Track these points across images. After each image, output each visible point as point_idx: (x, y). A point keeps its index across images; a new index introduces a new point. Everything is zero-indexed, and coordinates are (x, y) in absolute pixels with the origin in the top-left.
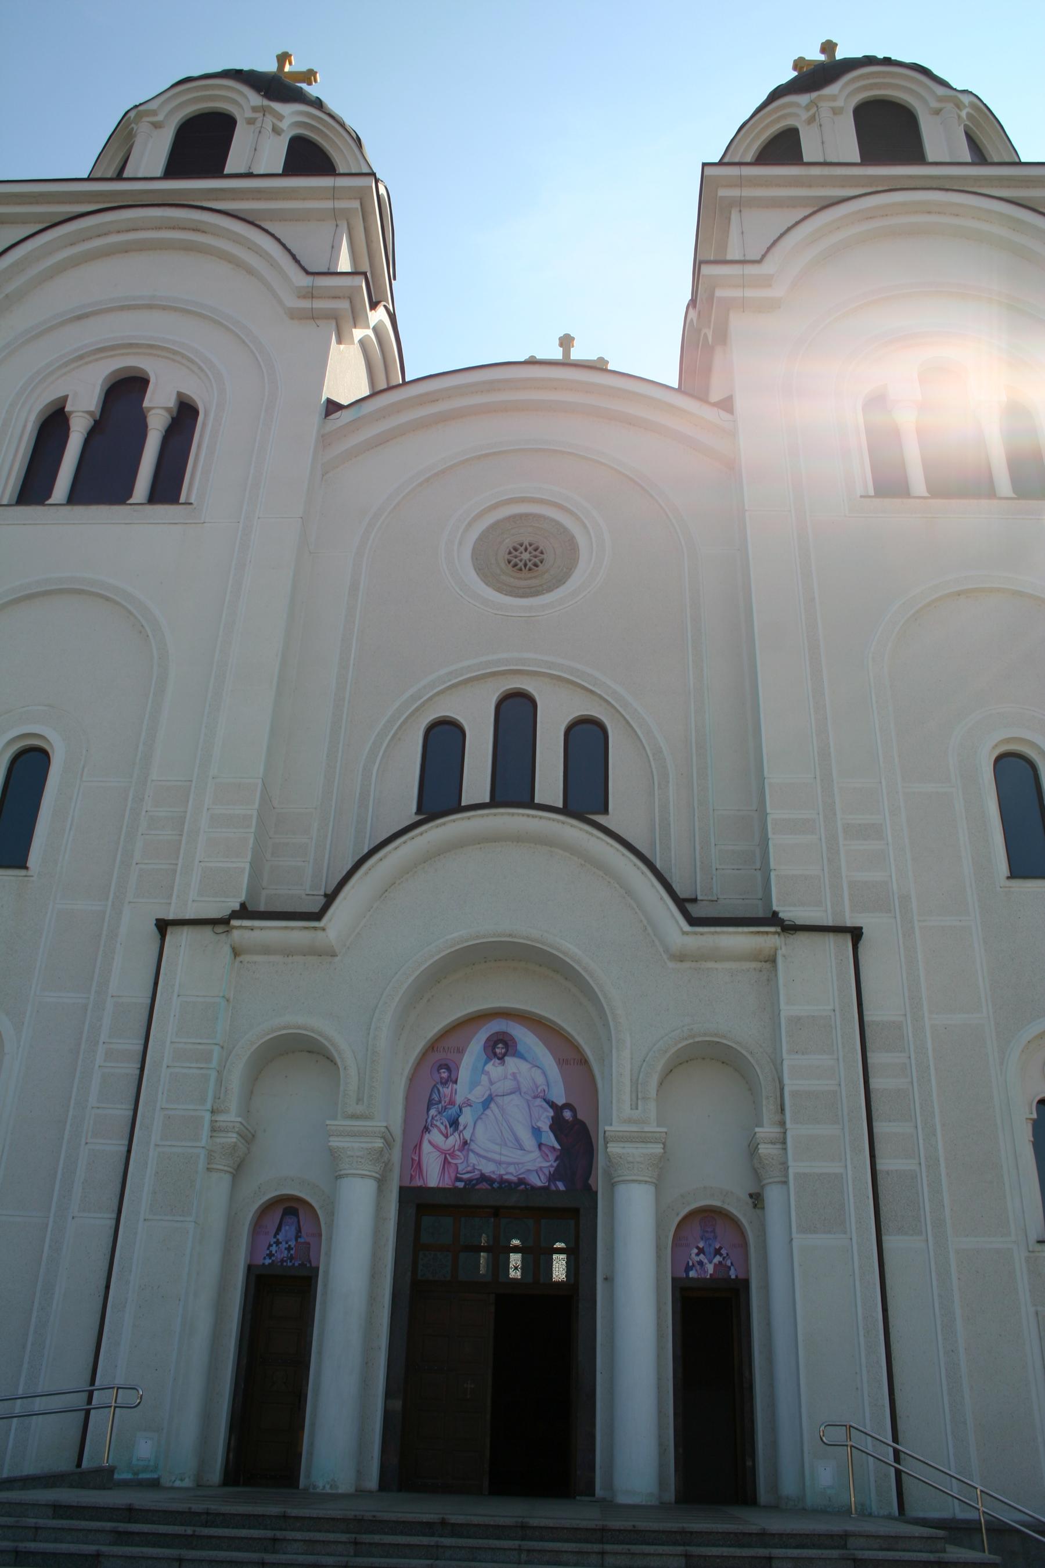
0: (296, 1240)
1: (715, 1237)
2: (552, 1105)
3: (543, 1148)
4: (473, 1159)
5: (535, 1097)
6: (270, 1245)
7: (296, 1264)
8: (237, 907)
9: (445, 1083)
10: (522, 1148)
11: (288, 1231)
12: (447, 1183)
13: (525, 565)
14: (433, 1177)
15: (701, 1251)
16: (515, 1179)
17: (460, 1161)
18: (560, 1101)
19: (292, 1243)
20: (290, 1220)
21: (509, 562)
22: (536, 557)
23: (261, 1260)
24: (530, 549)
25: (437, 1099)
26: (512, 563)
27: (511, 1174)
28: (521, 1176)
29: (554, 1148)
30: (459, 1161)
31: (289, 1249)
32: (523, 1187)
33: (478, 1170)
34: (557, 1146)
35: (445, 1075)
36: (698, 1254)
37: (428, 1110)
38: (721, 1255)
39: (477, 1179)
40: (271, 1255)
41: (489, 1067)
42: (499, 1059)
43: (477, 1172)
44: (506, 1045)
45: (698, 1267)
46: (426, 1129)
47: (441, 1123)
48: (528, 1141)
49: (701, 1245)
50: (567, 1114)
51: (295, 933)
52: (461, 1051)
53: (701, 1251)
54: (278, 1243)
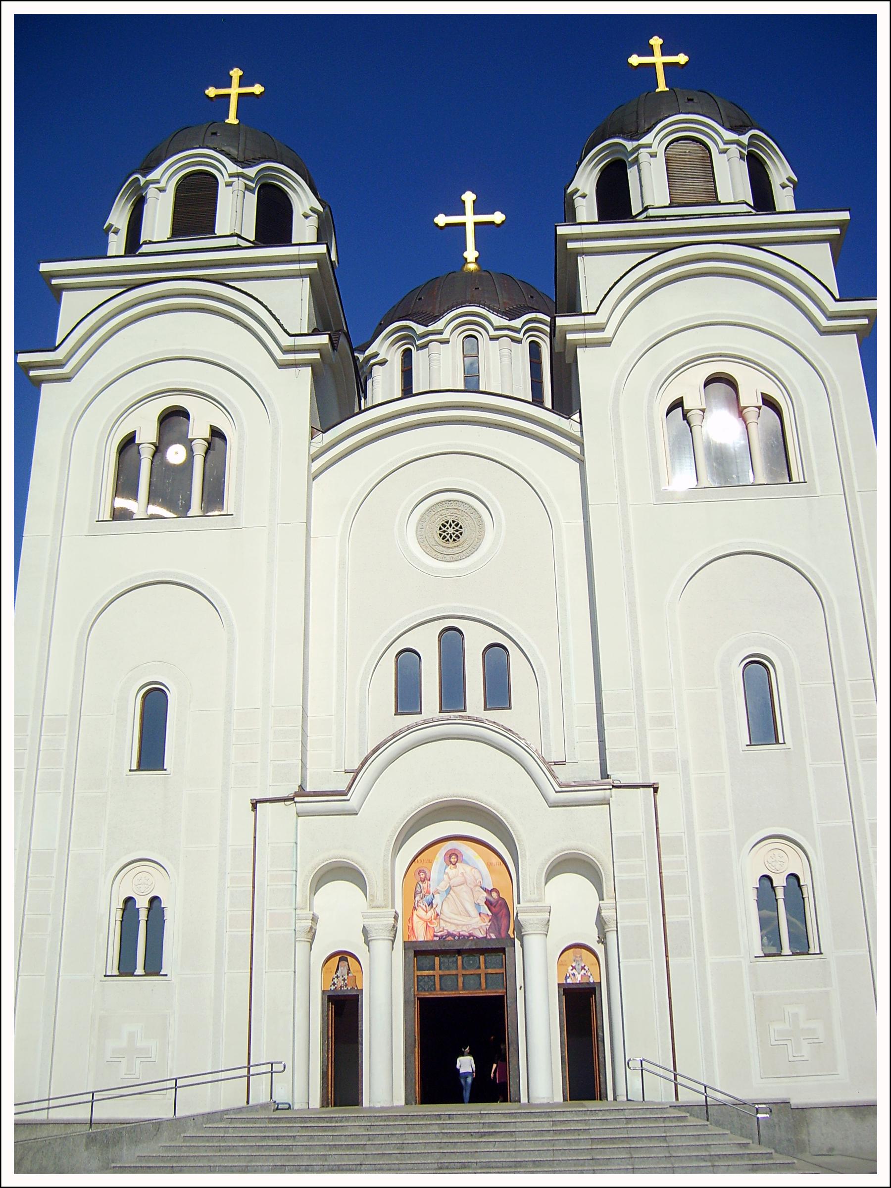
0: (348, 975)
1: (582, 960)
2: (486, 890)
3: (481, 915)
4: (442, 924)
5: (477, 886)
6: (333, 979)
7: (349, 988)
9: (423, 881)
10: (470, 916)
11: (343, 970)
12: (429, 938)
13: (451, 537)
14: (421, 935)
15: (574, 968)
16: (467, 934)
17: (435, 926)
19: (346, 977)
20: (343, 963)
21: (440, 535)
22: (457, 531)
24: (453, 525)
25: (419, 890)
26: (442, 536)
27: (465, 931)
28: (470, 932)
29: (488, 915)
30: (435, 925)
31: (344, 980)
32: (472, 938)
33: (447, 930)
34: (490, 914)
35: (423, 876)
36: (572, 970)
37: (415, 897)
38: (585, 969)
39: (446, 935)
40: (334, 984)
41: (448, 870)
42: (453, 865)
43: (445, 931)
45: (572, 977)
46: (415, 908)
47: (423, 904)
48: (473, 912)
49: (574, 965)
52: (431, 862)
53: (574, 968)
54: (337, 977)
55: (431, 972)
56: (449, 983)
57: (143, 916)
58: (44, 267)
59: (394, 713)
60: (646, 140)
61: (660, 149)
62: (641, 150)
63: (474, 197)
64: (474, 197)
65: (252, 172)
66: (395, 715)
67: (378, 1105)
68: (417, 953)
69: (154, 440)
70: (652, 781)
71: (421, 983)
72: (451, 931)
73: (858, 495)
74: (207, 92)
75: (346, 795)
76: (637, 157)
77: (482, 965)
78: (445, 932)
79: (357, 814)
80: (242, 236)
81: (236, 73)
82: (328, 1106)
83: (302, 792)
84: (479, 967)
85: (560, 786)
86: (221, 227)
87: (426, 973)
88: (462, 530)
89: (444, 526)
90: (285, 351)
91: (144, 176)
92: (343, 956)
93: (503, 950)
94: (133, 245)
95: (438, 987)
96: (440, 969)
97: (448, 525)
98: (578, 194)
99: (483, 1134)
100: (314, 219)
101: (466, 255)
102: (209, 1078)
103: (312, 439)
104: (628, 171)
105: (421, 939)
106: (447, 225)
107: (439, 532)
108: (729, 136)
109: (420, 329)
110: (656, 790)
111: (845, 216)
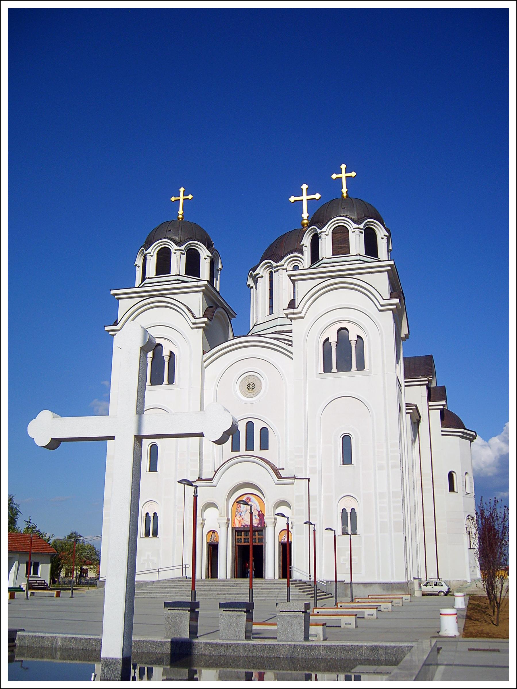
2: (258, 511)
8: (197, 479)
9: (238, 508)
11: (213, 536)
12: (240, 526)
14: (237, 525)
15: (284, 537)
18: (259, 510)
30: (242, 522)
34: (259, 519)
40: (211, 540)
44: (249, 500)
46: (236, 516)
47: (238, 515)
50: (261, 512)
51: (208, 483)
53: (284, 537)
55: (241, 537)
56: (247, 540)
57: (152, 519)
58: (112, 292)
59: (231, 451)
60: (324, 229)
62: (322, 233)
63: (307, 186)
64: (307, 186)
65: (183, 248)
66: (231, 452)
67: (221, 578)
68: (236, 531)
71: (241, 540)
72: (247, 524)
74: (171, 199)
75: (212, 481)
76: (321, 236)
77: (257, 535)
78: (245, 524)
79: (216, 486)
80: (180, 275)
81: (182, 190)
82: (208, 578)
84: (256, 536)
85: (278, 478)
87: (240, 537)
88: (254, 386)
89: (249, 384)
90: (193, 324)
91: (146, 251)
92: (214, 532)
93: (263, 530)
94: (144, 278)
95: (243, 542)
96: (244, 536)
97: (250, 384)
98: (304, 246)
99: (233, 586)
100: (209, 259)
101: (303, 215)
102: (171, 568)
103: (204, 355)
104: (319, 240)
105: (237, 526)
106: (295, 201)
107: (247, 387)
108: (356, 226)
109: (274, 264)
110: (309, 481)
111: (392, 262)
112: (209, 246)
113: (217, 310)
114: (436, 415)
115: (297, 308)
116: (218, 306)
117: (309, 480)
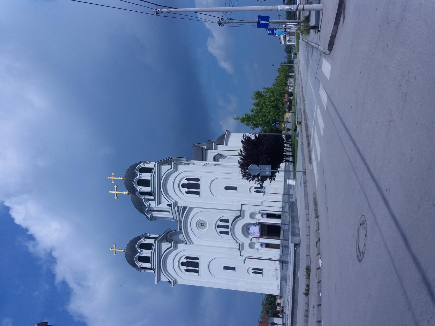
14: (259, 234)
23: (265, 247)
48: (256, 227)
57: (255, 271)
61: (140, 187)
65: (139, 251)
69: (186, 267)
70: (241, 205)
73: (202, 170)
83: (239, 249)
86: (150, 256)
87: (264, 234)
108: (138, 177)
112: (139, 238)
113: (169, 237)
114: (219, 147)
115: (172, 204)
116: (167, 236)
117: (242, 205)
